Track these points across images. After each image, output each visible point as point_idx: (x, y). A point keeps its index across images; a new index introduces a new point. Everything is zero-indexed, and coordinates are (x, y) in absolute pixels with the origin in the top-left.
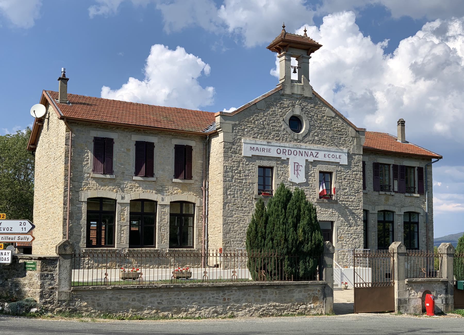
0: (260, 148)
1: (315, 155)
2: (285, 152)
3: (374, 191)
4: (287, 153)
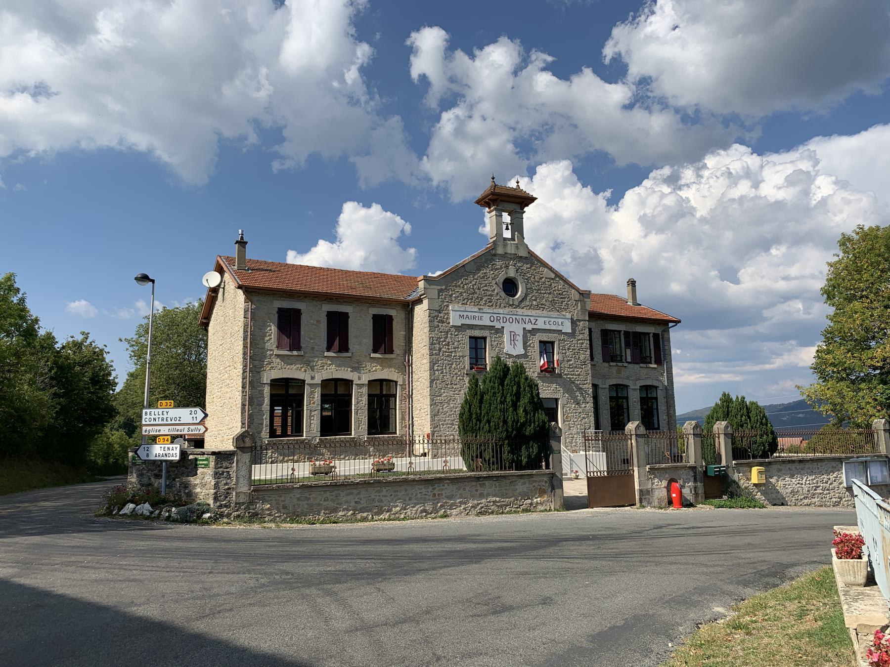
1: (533, 322)
3: (603, 362)
4: (501, 321)
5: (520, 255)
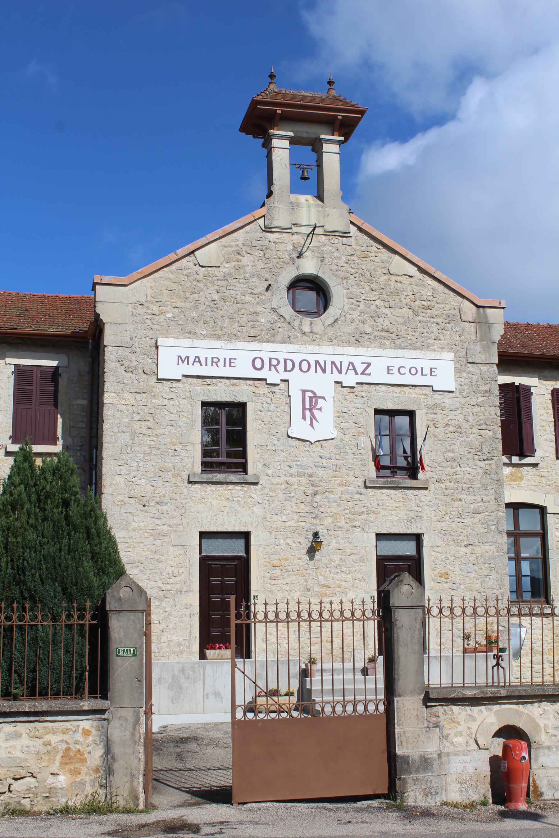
0: (206, 358)
1: (360, 369)
2: (275, 366)
4: (281, 367)
5: (327, 228)
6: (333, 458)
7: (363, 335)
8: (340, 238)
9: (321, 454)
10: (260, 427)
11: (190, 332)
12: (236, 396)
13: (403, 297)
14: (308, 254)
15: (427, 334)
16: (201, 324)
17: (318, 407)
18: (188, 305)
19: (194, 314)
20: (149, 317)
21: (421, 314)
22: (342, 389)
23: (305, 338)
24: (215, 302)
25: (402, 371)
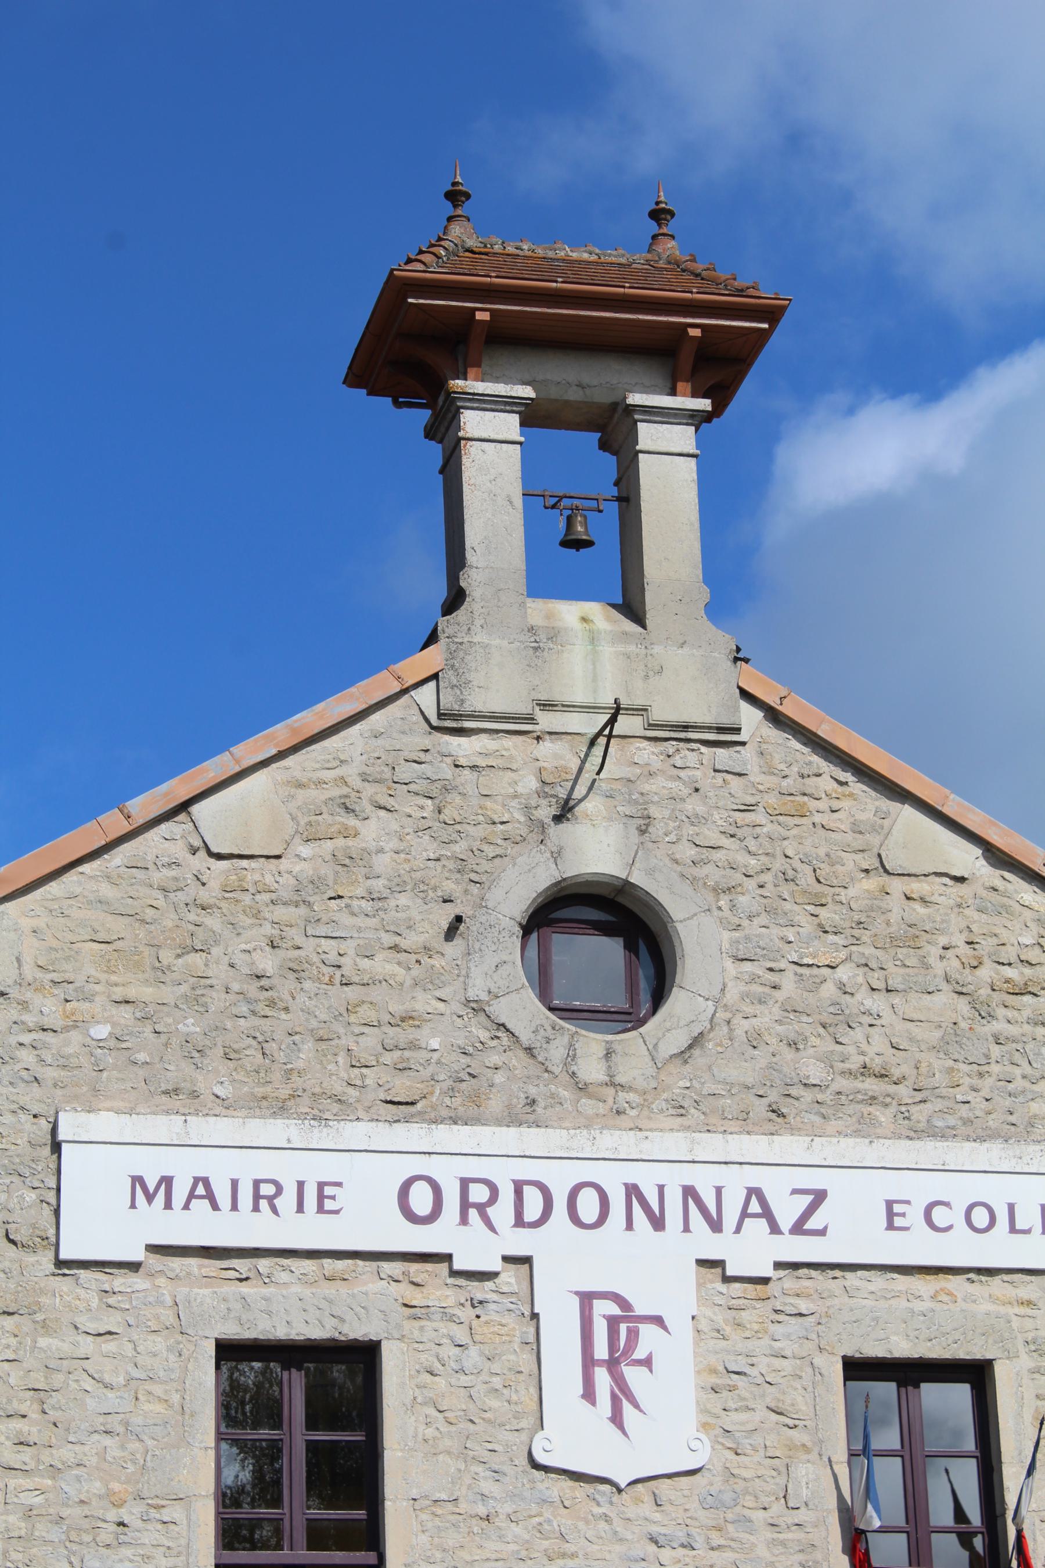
0: (235, 1184)
1: (787, 1212)
2: (481, 1208)
4: (502, 1212)
5: (658, 715)
6: (699, 1542)
7: (793, 1091)
8: (703, 749)
9: (655, 1529)
10: (430, 1432)
11: (176, 1091)
12: (342, 1320)
13: (935, 951)
14: (591, 806)
15: (1027, 1084)
16: (214, 1060)
17: (640, 1354)
18: (169, 994)
19: (191, 1026)
20: (26, 1038)
21: (1001, 1012)
22: (723, 1288)
23: (587, 1105)
24: (264, 982)
25: (939, 1216)
